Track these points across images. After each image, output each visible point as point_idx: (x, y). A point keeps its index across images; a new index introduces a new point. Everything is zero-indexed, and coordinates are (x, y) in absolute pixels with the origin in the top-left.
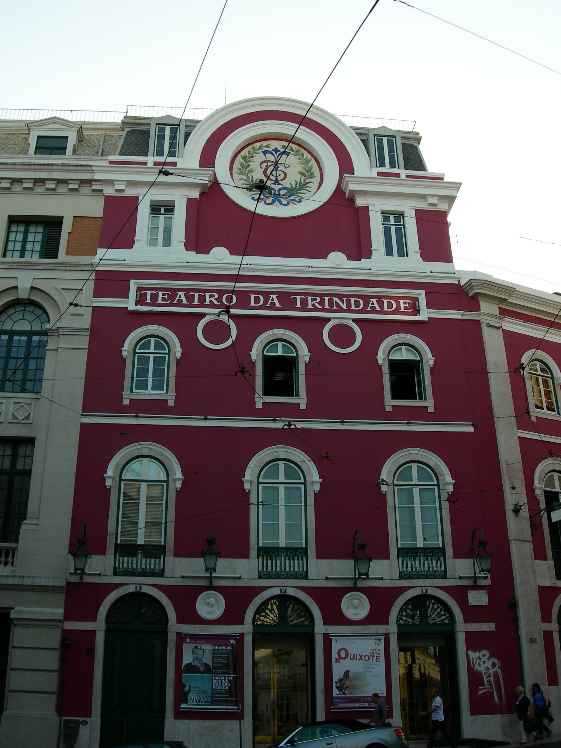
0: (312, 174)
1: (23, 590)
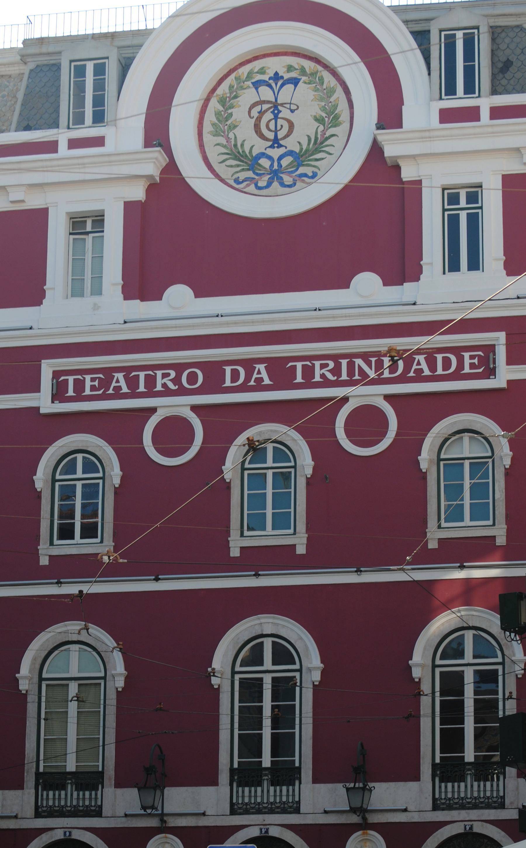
0: (337, 117)
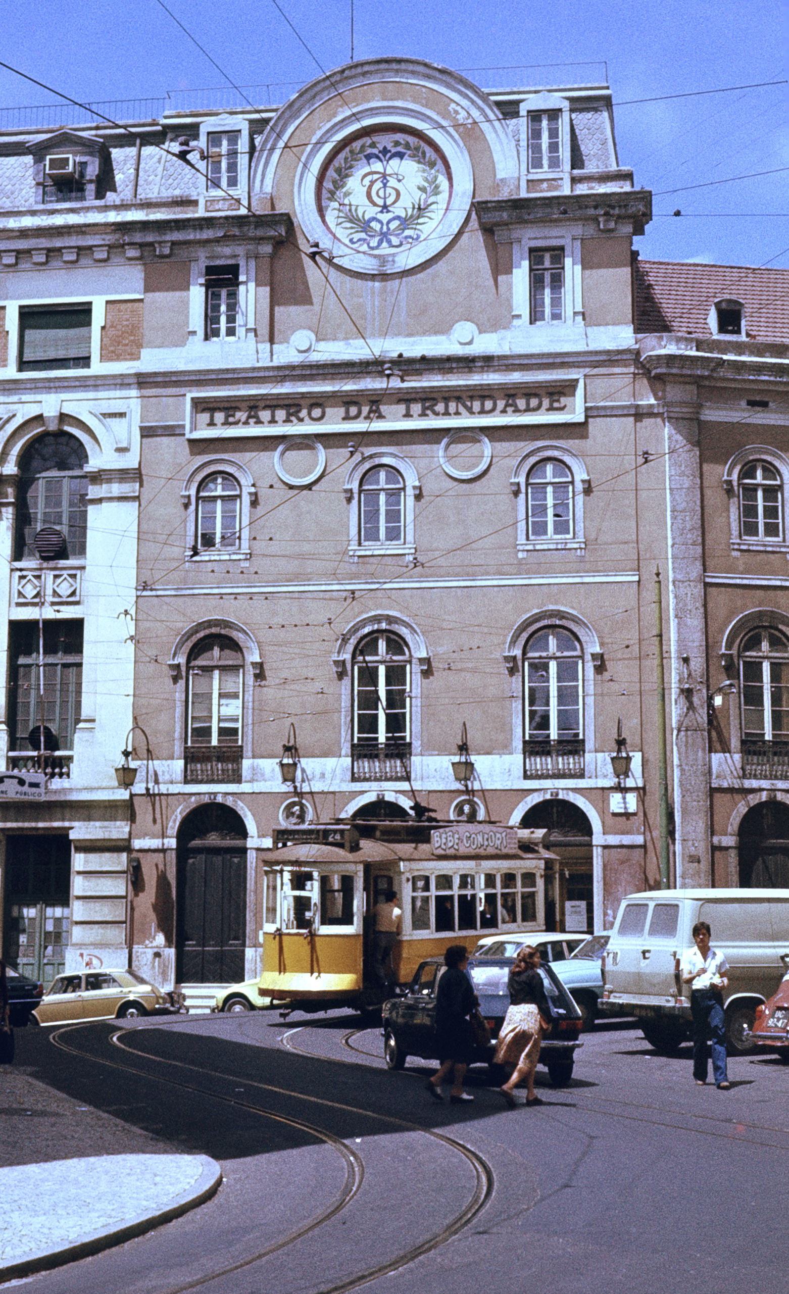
0: (437, 187)
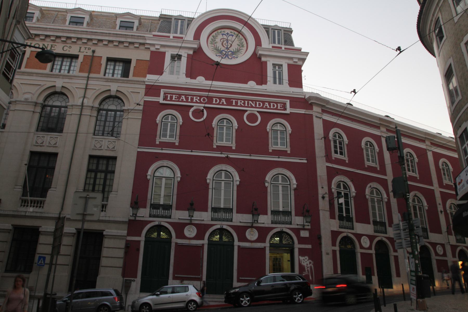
0: (243, 45)
1: (109, 223)
